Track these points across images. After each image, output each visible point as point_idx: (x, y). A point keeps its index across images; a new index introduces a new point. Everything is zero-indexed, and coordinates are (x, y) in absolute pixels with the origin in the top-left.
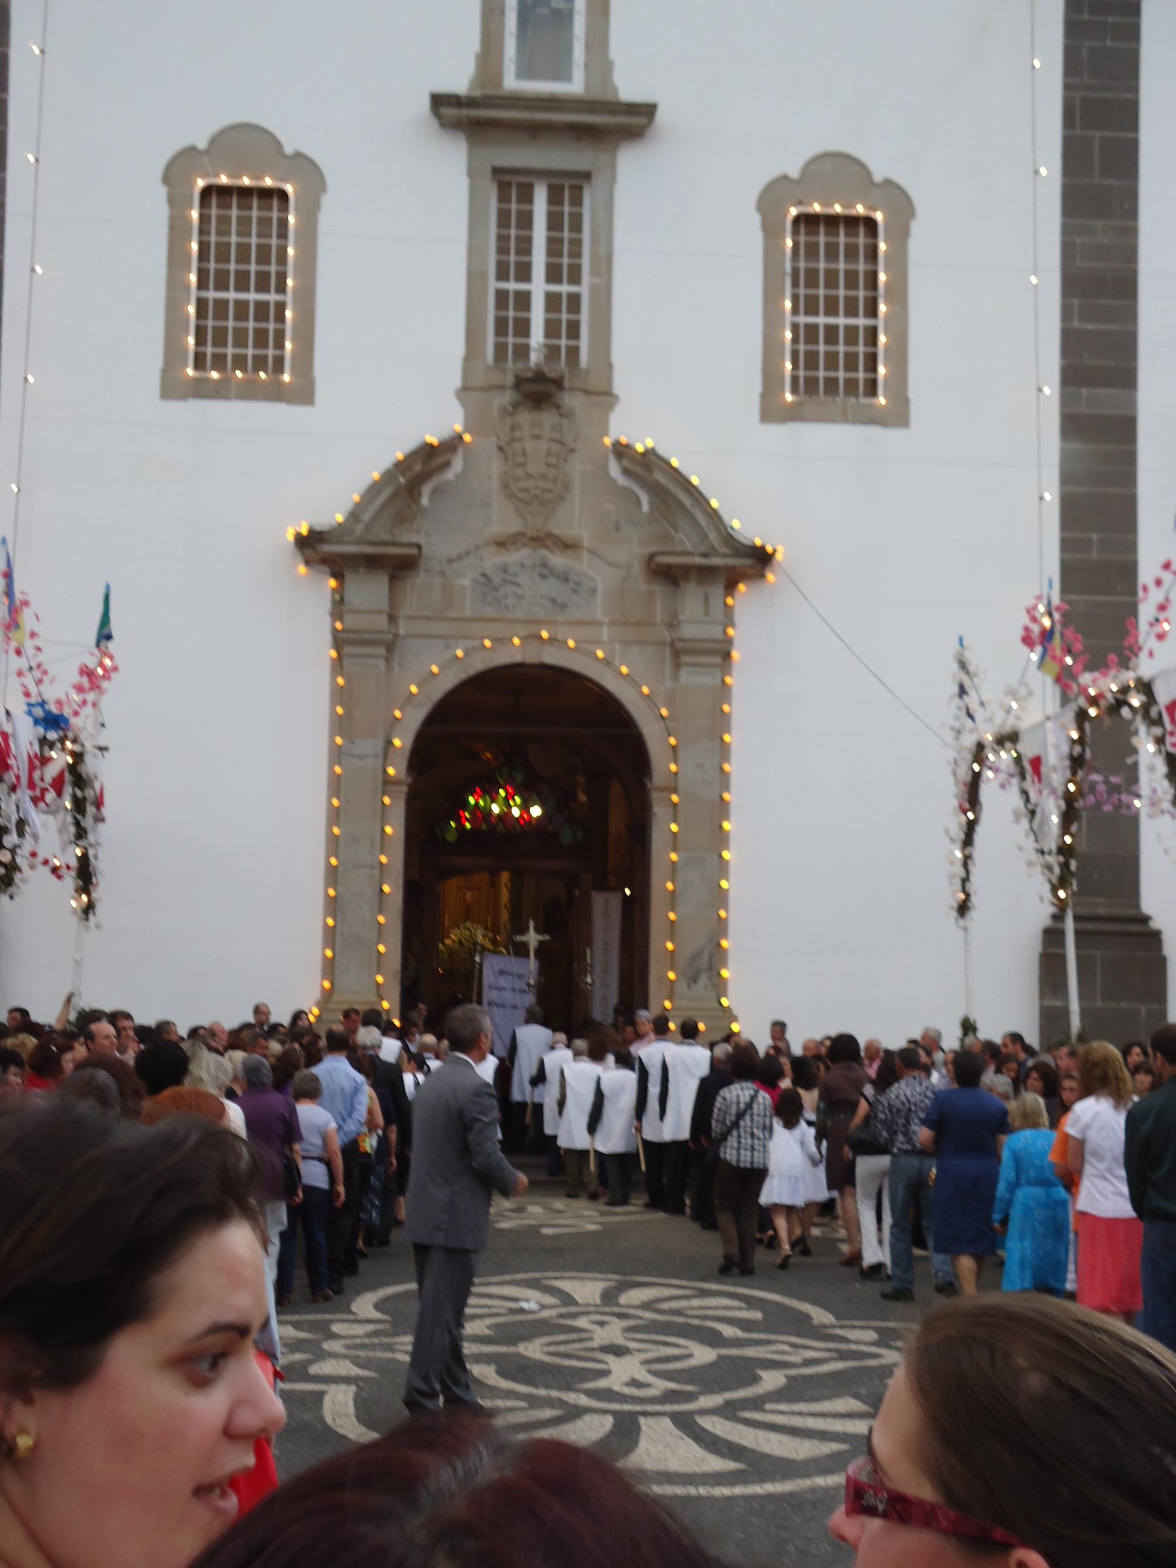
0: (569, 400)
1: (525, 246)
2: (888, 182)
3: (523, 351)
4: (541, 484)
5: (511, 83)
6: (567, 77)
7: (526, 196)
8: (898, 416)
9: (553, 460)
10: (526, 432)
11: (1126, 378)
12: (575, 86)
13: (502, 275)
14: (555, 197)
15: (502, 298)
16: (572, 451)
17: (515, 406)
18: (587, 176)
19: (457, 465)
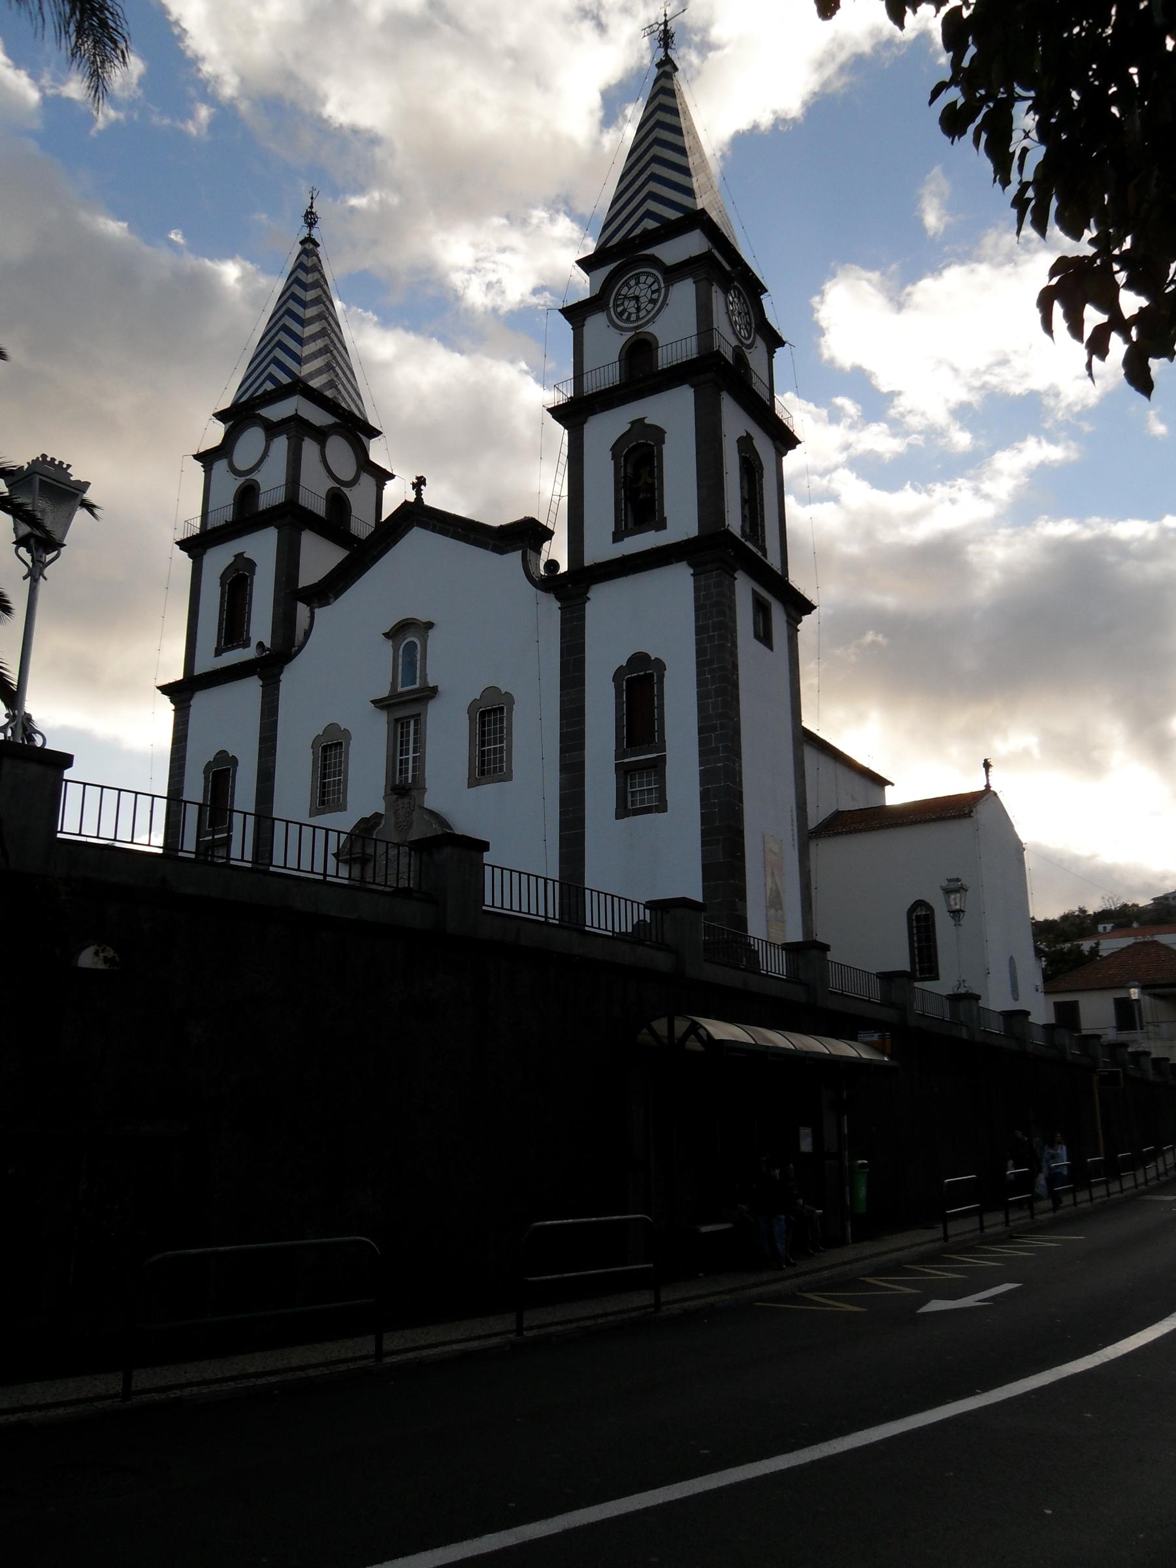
0: (414, 793)
1: (408, 741)
2: (506, 692)
3: (407, 778)
4: (404, 823)
5: (400, 689)
6: (415, 684)
7: (409, 723)
8: (508, 777)
9: (407, 815)
10: (400, 807)
11: (581, 747)
12: (417, 686)
13: (401, 755)
14: (416, 724)
15: (401, 760)
16: (413, 810)
17: (397, 799)
18: (419, 715)
19: (383, 822)
